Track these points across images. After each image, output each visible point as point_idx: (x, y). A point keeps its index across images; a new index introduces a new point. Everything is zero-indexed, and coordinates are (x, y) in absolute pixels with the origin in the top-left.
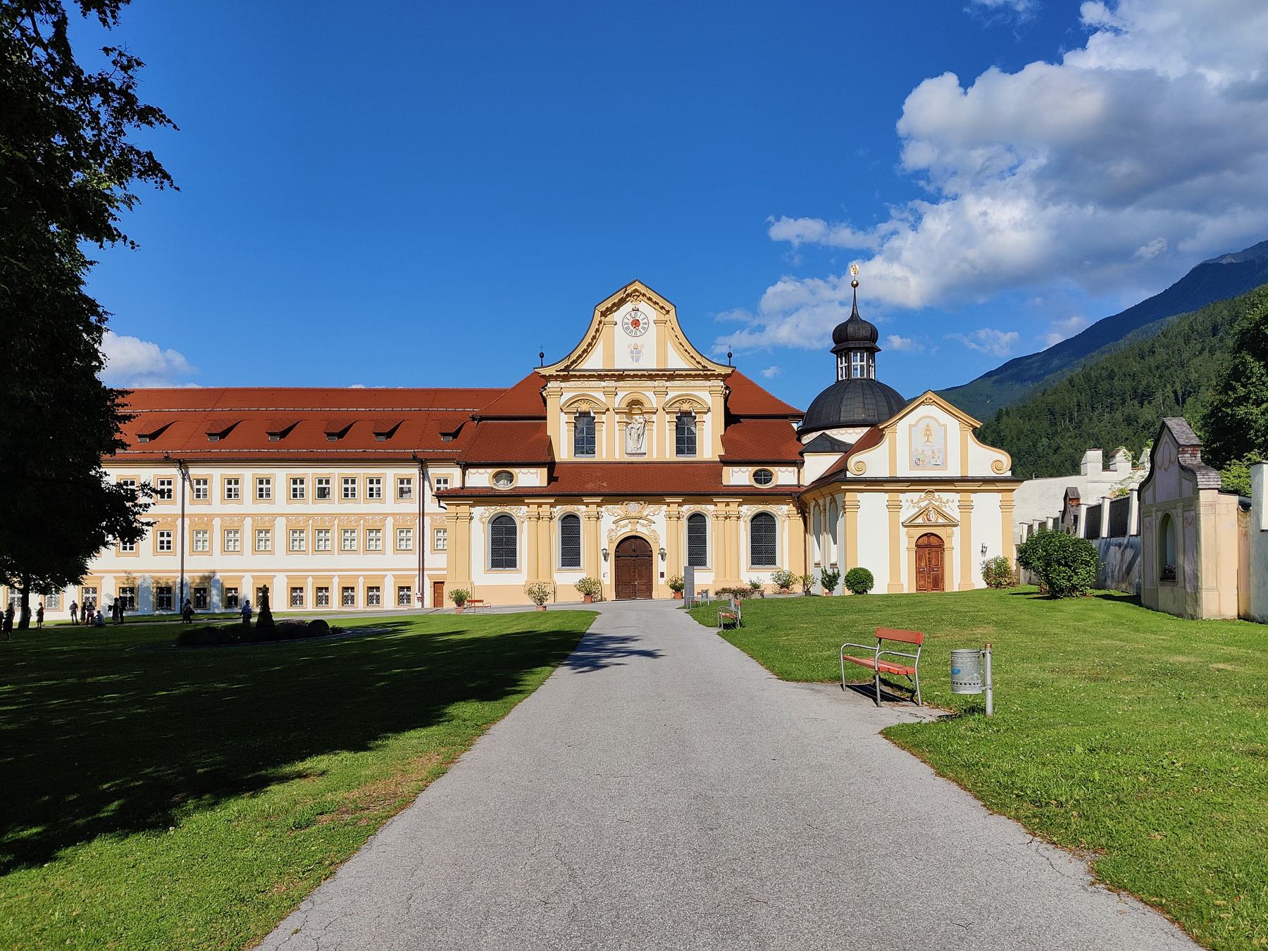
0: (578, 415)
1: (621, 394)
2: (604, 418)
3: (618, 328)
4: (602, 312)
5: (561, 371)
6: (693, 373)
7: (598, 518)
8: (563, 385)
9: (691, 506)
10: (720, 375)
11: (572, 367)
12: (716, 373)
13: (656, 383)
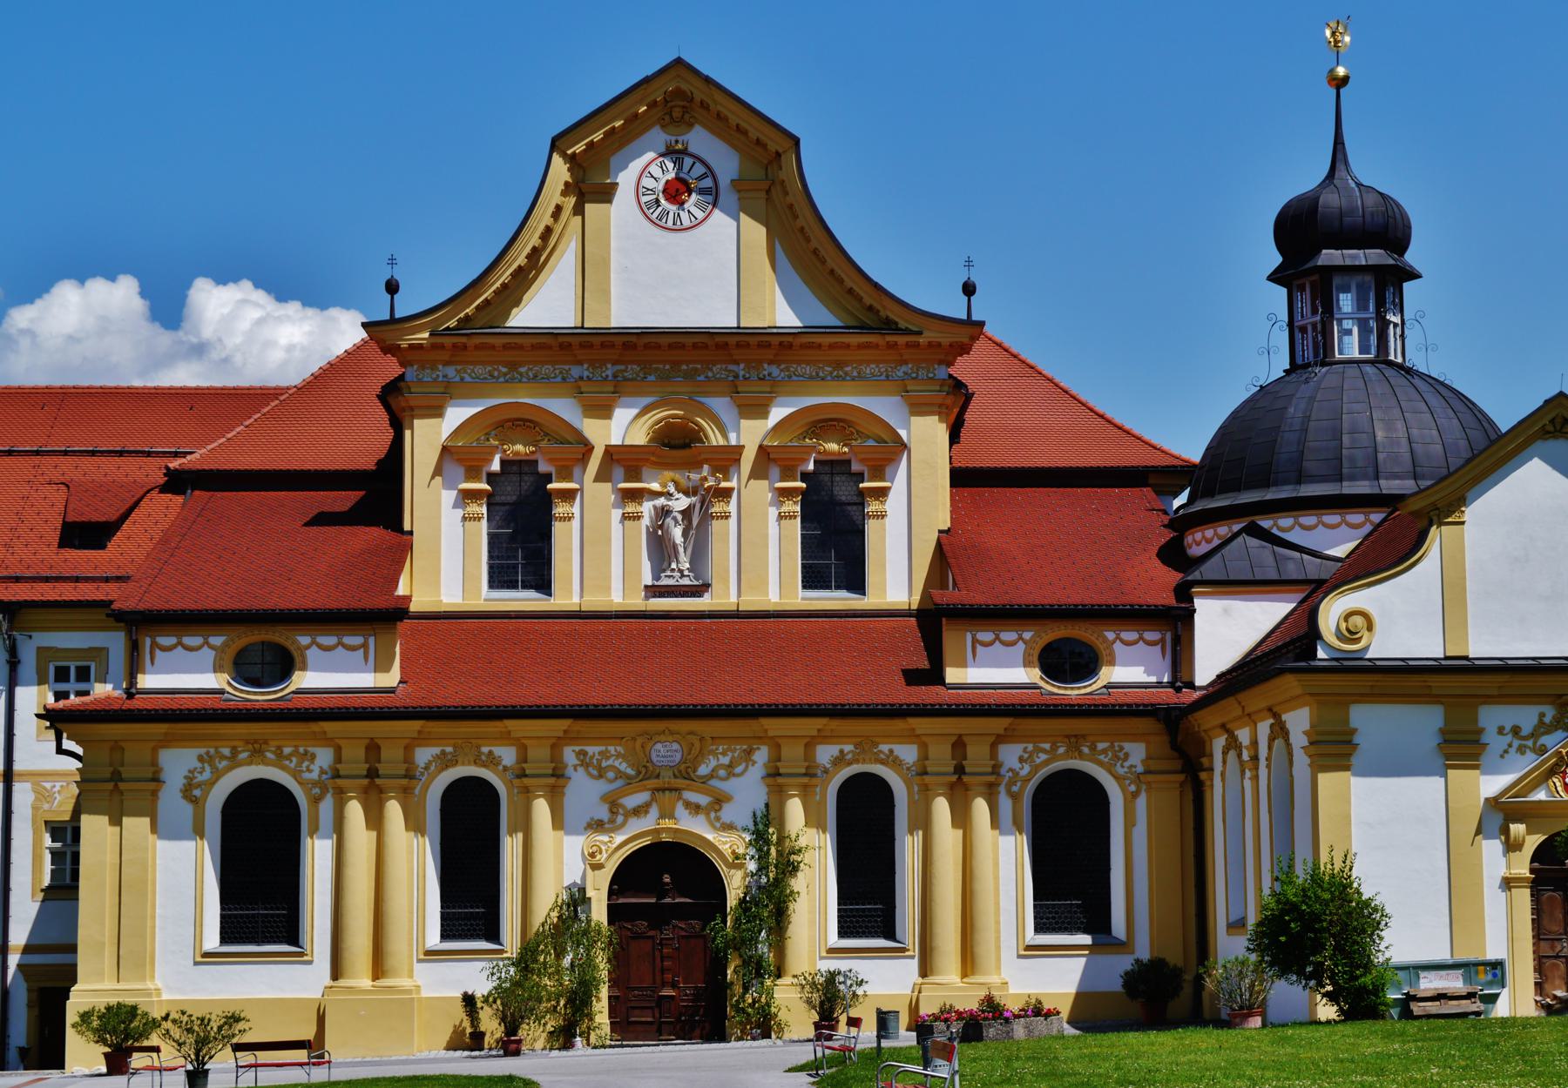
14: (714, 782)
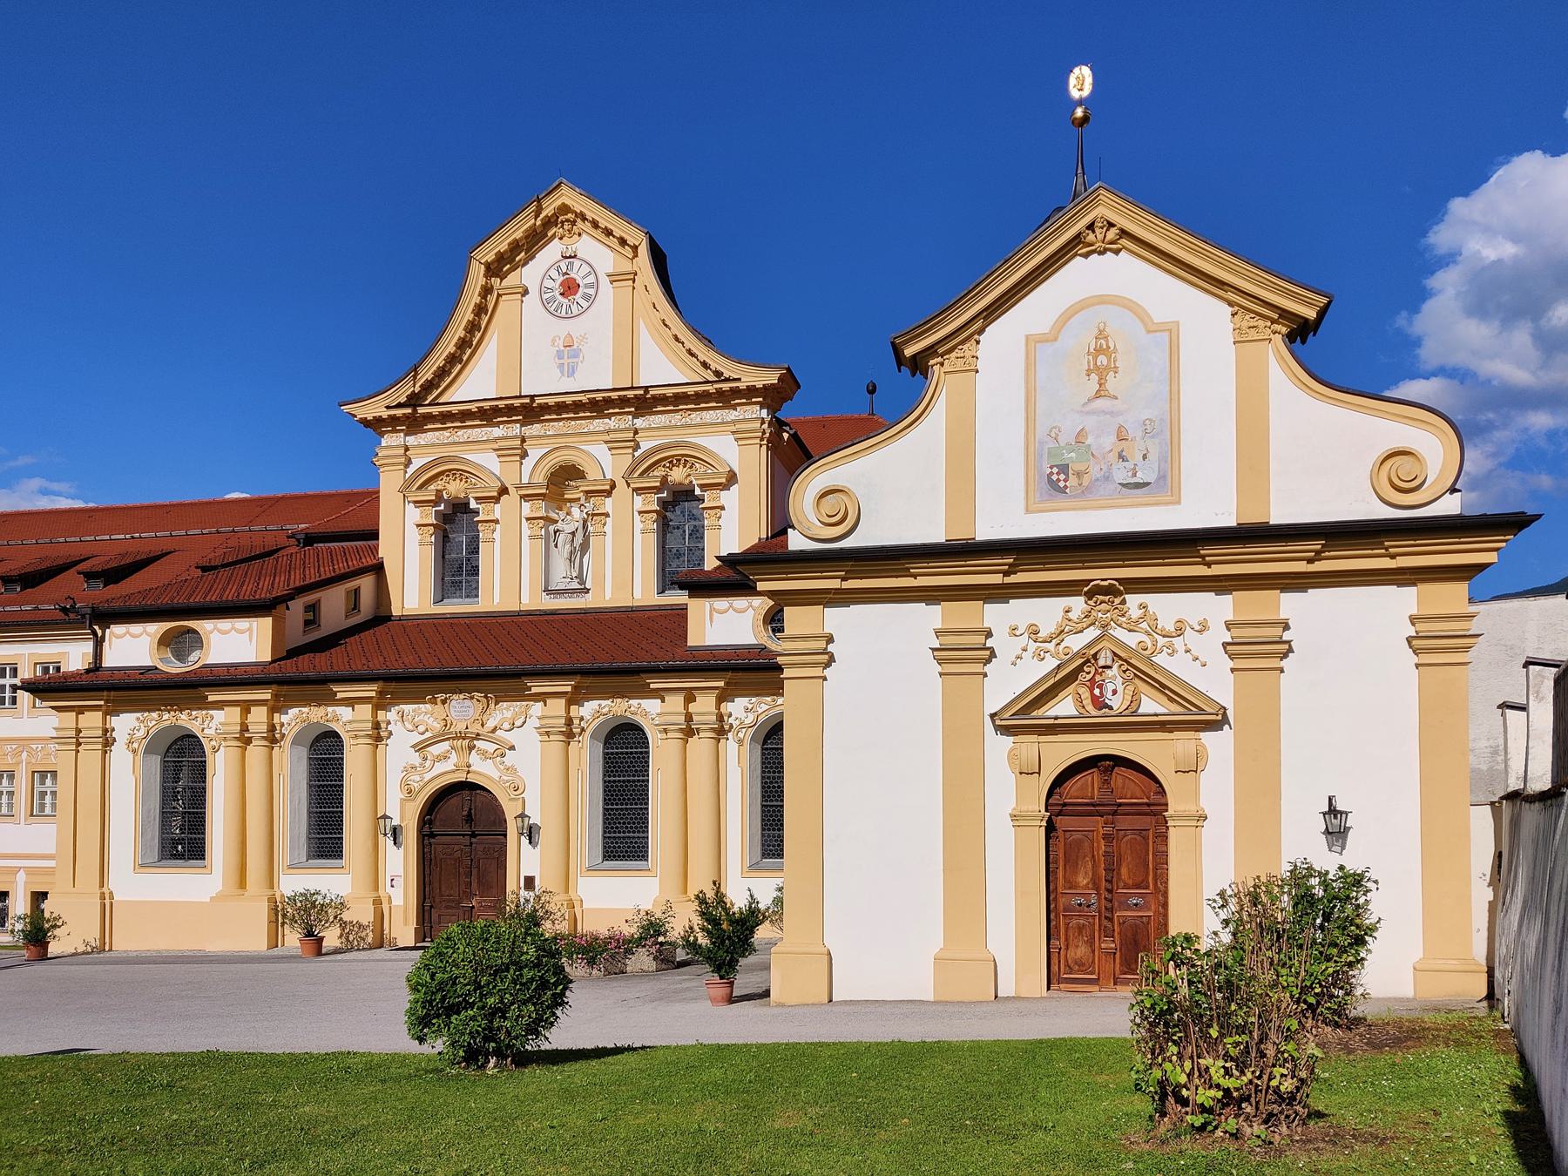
0: (442, 507)
1: (534, 454)
2: (497, 511)
3: (532, 300)
4: (488, 266)
5: (399, 406)
6: (691, 390)
7: (378, 739)
8: (411, 440)
9: (604, 703)
10: (751, 392)
11: (430, 399)
12: (742, 386)
13: (612, 423)
14: (498, 732)
